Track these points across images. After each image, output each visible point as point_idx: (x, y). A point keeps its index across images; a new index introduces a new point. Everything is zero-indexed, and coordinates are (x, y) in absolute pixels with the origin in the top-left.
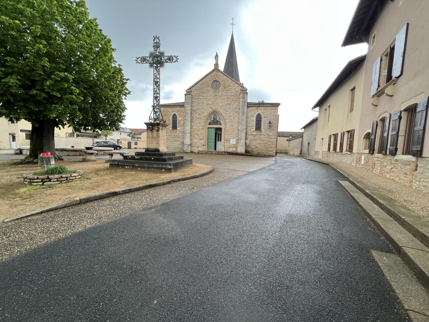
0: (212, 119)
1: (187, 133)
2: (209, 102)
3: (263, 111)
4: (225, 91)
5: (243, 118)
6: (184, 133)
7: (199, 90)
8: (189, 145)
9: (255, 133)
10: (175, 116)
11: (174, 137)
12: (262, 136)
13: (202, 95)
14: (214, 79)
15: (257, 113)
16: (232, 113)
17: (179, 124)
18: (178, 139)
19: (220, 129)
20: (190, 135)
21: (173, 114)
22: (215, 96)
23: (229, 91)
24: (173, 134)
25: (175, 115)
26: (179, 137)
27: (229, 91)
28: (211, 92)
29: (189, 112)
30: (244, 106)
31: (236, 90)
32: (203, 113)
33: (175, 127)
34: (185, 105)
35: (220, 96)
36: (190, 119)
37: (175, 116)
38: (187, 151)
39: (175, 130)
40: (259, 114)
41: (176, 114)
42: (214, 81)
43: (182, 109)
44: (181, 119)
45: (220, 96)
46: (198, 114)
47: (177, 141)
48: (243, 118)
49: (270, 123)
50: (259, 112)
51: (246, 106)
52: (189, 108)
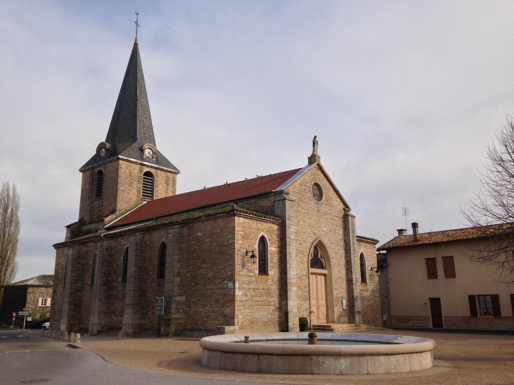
11: (262, 295)
13: (303, 205)
22: (318, 211)
24: (261, 286)
25: (263, 240)
28: (313, 203)
39: (264, 277)
40: (362, 253)
41: (266, 236)
50: (362, 250)
51: (355, 240)
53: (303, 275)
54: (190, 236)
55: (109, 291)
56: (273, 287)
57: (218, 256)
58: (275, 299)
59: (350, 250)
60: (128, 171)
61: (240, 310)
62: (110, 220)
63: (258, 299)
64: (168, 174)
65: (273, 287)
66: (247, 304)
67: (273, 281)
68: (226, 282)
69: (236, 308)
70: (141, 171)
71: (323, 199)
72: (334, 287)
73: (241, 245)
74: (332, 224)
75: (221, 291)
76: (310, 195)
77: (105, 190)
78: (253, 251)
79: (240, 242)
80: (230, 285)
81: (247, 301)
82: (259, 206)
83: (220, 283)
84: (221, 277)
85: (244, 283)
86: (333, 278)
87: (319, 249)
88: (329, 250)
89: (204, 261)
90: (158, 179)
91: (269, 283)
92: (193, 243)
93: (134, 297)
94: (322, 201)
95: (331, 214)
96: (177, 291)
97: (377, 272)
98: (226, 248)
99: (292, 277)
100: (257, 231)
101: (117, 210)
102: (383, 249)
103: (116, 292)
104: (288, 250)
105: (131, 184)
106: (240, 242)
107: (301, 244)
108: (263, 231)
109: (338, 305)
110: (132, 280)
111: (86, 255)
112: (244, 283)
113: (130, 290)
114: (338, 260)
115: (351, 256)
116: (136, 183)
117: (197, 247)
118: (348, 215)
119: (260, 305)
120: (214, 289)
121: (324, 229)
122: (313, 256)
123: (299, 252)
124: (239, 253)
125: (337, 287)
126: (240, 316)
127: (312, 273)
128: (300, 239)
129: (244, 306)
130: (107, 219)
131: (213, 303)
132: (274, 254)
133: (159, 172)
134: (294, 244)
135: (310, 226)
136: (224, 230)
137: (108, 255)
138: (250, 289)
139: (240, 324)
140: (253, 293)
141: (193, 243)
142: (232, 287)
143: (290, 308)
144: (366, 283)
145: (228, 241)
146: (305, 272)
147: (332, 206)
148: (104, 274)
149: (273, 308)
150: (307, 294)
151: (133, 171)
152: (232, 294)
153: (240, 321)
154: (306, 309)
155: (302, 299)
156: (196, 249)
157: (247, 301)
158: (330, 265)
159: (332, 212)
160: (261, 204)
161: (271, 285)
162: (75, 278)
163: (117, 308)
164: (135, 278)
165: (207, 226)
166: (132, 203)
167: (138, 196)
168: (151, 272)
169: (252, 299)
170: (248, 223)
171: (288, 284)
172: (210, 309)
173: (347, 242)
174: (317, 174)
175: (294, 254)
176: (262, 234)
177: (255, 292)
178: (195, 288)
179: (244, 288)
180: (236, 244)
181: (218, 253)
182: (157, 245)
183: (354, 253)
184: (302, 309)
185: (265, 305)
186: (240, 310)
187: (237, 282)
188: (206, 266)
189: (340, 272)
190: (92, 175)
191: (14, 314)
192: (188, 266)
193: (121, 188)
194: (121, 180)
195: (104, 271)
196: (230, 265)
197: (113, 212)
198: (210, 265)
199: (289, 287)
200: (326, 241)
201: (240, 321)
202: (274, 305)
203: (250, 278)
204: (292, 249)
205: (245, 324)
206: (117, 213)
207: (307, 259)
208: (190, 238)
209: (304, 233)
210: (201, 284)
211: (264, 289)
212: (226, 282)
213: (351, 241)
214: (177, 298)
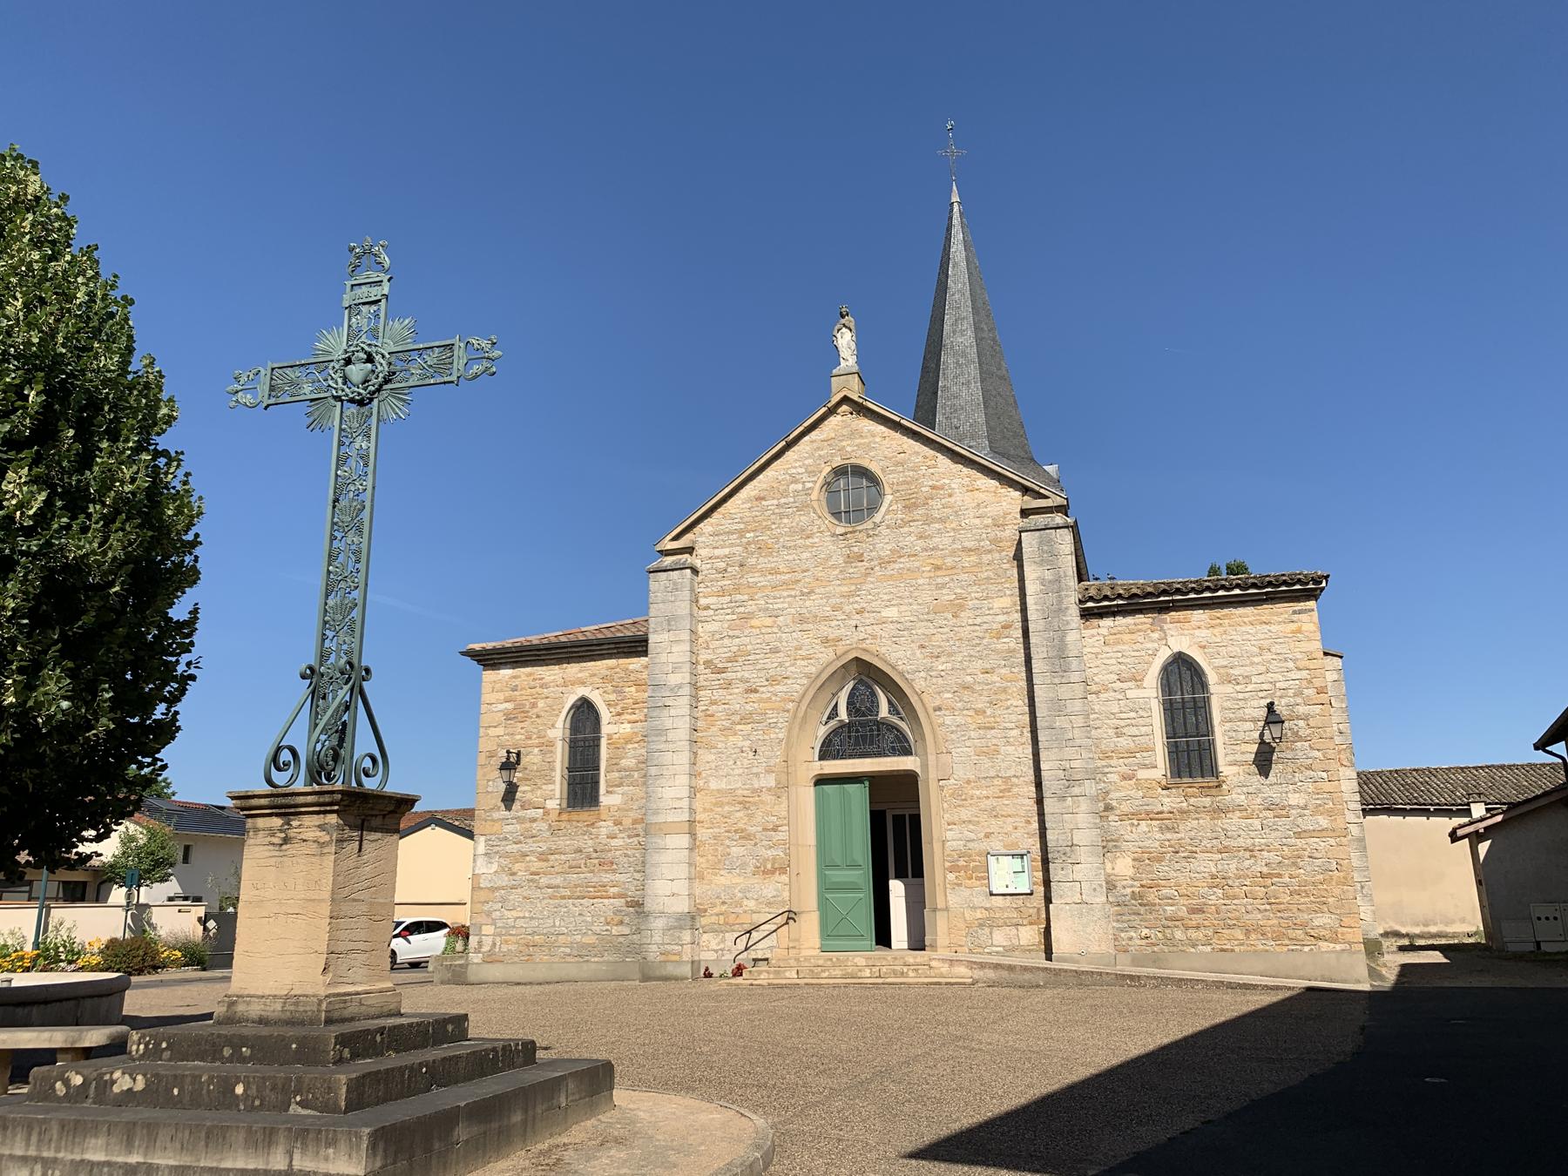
0: (843, 715)
1: (667, 829)
3: (1204, 633)
4: (915, 528)
5: (1064, 692)
6: (644, 829)
7: (742, 533)
8: (680, 918)
9: (1170, 801)
10: (585, 714)
12: (1233, 821)
14: (837, 462)
15: (1164, 655)
16: (979, 664)
17: (614, 764)
18: (607, 878)
19: (908, 782)
20: (684, 840)
21: (571, 700)
22: (849, 559)
23: (942, 520)
26: (607, 864)
27: (942, 520)
29: (681, 678)
30: (1061, 611)
31: (993, 510)
32: (772, 681)
33: (583, 788)
34: (652, 638)
35: (884, 563)
36: (684, 725)
37: (585, 714)
38: (671, 970)
39: (585, 815)
41: (596, 698)
42: (840, 472)
43: (635, 663)
44: (626, 728)
45: (884, 563)
46: (738, 689)
47: (600, 892)
48: (1064, 692)
49: (1272, 717)
51: (1074, 611)
52: (680, 652)
53: (757, 792)
56: (614, 842)
61: (489, 914)
63: (558, 880)
66: (514, 897)
67: (617, 823)
71: (883, 509)
79: (500, 731)
85: (506, 839)
91: (604, 831)
94: (878, 517)
106: (500, 731)
107: (756, 691)
108: (583, 683)
112: (506, 839)
119: (563, 898)
121: (892, 613)
126: (488, 930)
128: (746, 675)
129: (504, 900)
135: (802, 621)
139: (485, 949)
140: (538, 866)
153: (488, 942)
174: (853, 434)
176: (582, 691)
179: (507, 855)
186: (489, 914)
187: (483, 839)
189: (991, 753)
201: (488, 942)
202: (620, 896)
203: (528, 825)
205: (504, 949)
209: (775, 651)
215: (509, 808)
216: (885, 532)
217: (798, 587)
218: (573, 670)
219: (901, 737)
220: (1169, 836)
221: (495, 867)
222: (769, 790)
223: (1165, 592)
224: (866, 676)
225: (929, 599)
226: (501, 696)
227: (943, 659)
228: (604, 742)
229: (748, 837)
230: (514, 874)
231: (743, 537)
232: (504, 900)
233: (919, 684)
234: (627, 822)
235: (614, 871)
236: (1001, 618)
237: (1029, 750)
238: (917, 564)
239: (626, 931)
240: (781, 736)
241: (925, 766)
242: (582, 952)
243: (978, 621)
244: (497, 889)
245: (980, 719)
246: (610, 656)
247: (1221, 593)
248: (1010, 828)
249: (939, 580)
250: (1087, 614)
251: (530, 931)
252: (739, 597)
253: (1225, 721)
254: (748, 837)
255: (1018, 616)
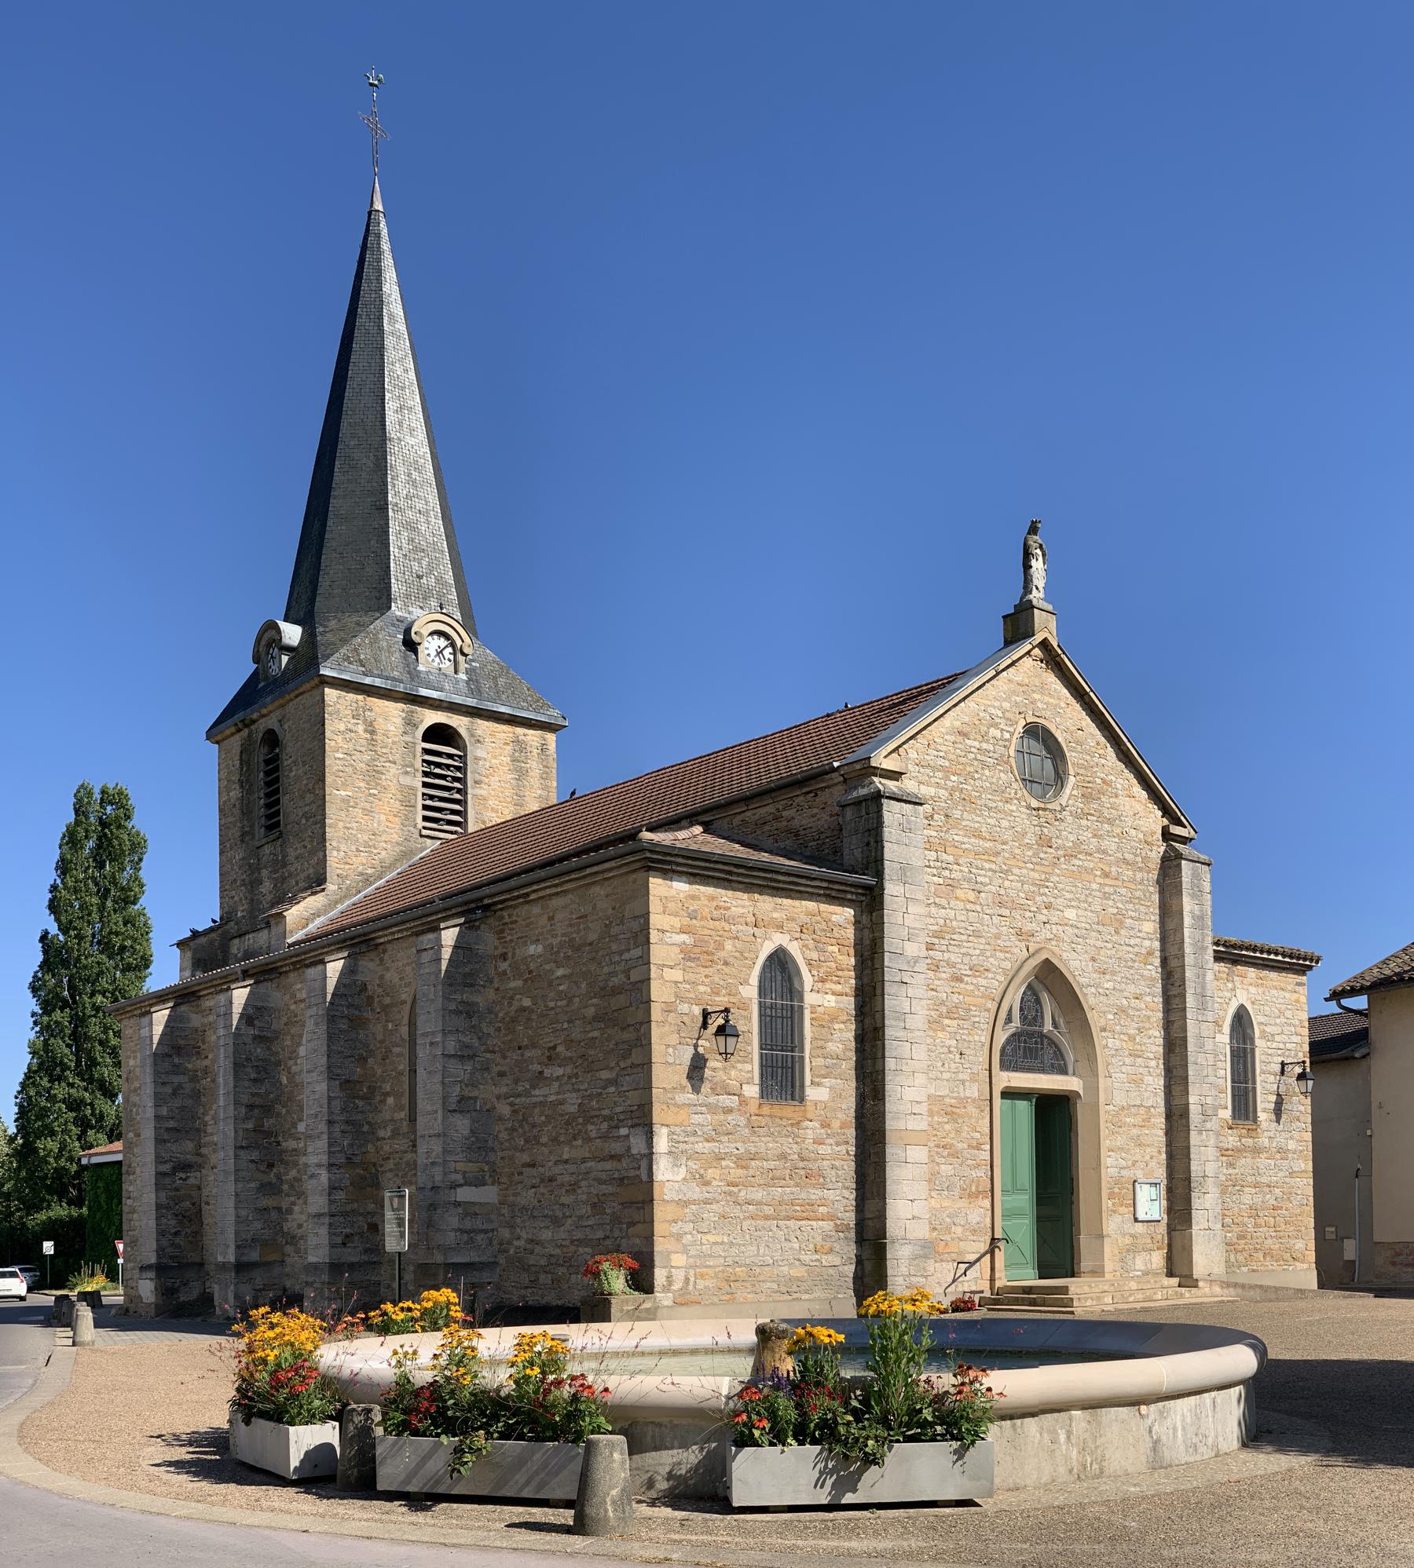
2: (1011, 885)
11: (774, 1180)
13: (970, 820)
16: (1132, 988)
18: (815, 1194)
21: (767, 949)
24: (766, 1145)
25: (780, 966)
27: (1110, 821)
28: (1017, 812)
39: (789, 1110)
40: (1242, 1006)
41: (794, 949)
44: (830, 1001)
47: (808, 1211)
53: (963, 1101)
54: (504, 957)
55: (271, 1166)
56: (823, 1150)
57: (596, 1034)
58: (841, 1198)
59: (1183, 996)
60: (361, 728)
61: (679, 1237)
62: (304, 917)
63: (759, 1195)
64: (520, 731)
65: (823, 1150)
66: (710, 1215)
67: (825, 1125)
68: (623, 1131)
69: (659, 1228)
70: (410, 723)
72: (1105, 1144)
73: (674, 986)
74: (1106, 896)
75: (608, 1165)
76: (1005, 778)
77: (291, 807)
78: (727, 1010)
79: (676, 975)
80: (637, 1145)
81: (707, 1202)
82: (789, 831)
83: (604, 1137)
84: (606, 1112)
86: (1102, 1109)
87: (1045, 997)
88: (1089, 999)
89: (551, 1058)
90: (480, 753)
92: (513, 984)
93: (333, 1188)
95: (1104, 852)
96: (460, 1166)
97: (1302, 1077)
98: (621, 1000)
99: (906, 1108)
100: (751, 930)
101: (331, 874)
102: (1353, 992)
103: (293, 1173)
104: (889, 1003)
105: (373, 774)
106: (676, 975)
107: (959, 979)
108: (780, 927)
109: (1122, 1210)
110: (323, 1127)
111: (204, 1043)
113: (319, 1166)
114: (1132, 1038)
115: (1185, 1018)
116: (393, 770)
117: (527, 1002)
118: (1179, 856)
120: (584, 1160)
121: (1071, 914)
122: (1016, 1023)
123: (944, 1014)
124: (671, 1017)
125: (1120, 1141)
126: (679, 1260)
127: (1009, 1094)
129: (697, 1219)
130: (293, 914)
131: (585, 1210)
132: (834, 1019)
133: (483, 726)
134: (920, 979)
136: (614, 931)
137: (259, 1039)
138: (719, 1158)
139: (676, 1286)
140: (737, 1173)
141: (513, 984)
142: (645, 1151)
143: (893, 1228)
144: (1255, 1120)
145: (627, 973)
146: (975, 1091)
147: (1110, 821)
148: (251, 1107)
149: (828, 1226)
150: (982, 1173)
151: (380, 724)
152: (644, 1178)
153: (679, 1276)
154: (974, 1232)
155: (957, 1192)
156: (524, 1009)
157: (707, 1202)
158: (1092, 1058)
159: (1110, 844)
160: (796, 823)
161: (819, 1142)
162: (171, 1124)
163: (300, 1226)
164: (330, 1122)
165: (559, 916)
166: (386, 851)
167: (408, 819)
168: (390, 1100)
169: (730, 1194)
170: (712, 898)
171: (890, 1137)
172: (579, 1235)
173: (1173, 963)
175: (917, 1021)
176: (778, 940)
177: (746, 1168)
178: (526, 1158)
180: (655, 986)
181: (594, 1018)
182: (404, 997)
183: (1202, 1007)
184: (959, 1230)
185: (789, 1218)
186: (679, 1237)
187: (665, 1130)
188: (560, 1071)
189: (1137, 1082)
190: (246, 751)
191: (121, 1247)
192: (501, 1074)
193: (337, 792)
194: (334, 759)
195: (245, 1099)
196: (633, 1066)
197: (317, 882)
198: (569, 1070)
199: (890, 1150)
200: (1075, 966)
201: (679, 1276)
202: (831, 1217)
204: (908, 1004)
205: (701, 1284)
206: (331, 887)
207: (985, 1038)
208: (504, 966)
209: (977, 934)
210: (544, 1140)
211: (783, 1157)
212: (623, 1131)
213: (1189, 960)
214: (464, 1194)
215: (696, 1090)
216: (1070, 819)
217: (1000, 859)
218: (767, 905)
219: (1059, 1054)
220: (1231, 1171)
221: (682, 1172)
222: (974, 1100)
223: (1247, 949)
224: (1049, 980)
225: (1099, 908)
226: (676, 922)
227: (1108, 977)
228: (807, 1015)
229: (955, 1155)
230: (707, 1183)
231: (947, 778)
232: (697, 1219)
233: (1092, 1001)
234: (836, 1124)
235: (823, 1187)
236: (1147, 943)
237: (1162, 1082)
238: (1092, 865)
239: (837, 1261)
240: (983, 1039)
241: (1093, 1088)
242: (790, 1288)
243: (1132, 942)
244: (686, 1204)
245: (1130, 1045)
246: (811, 896)
247: (1272, 957)
248: (1147, 1158)
249: (1107, 889)
250: (1219, 957)
251: (730, 1261)
252: (944, 857)
253: (1263, 1072)
254: (955, 1155)
255: (1157, 944)
